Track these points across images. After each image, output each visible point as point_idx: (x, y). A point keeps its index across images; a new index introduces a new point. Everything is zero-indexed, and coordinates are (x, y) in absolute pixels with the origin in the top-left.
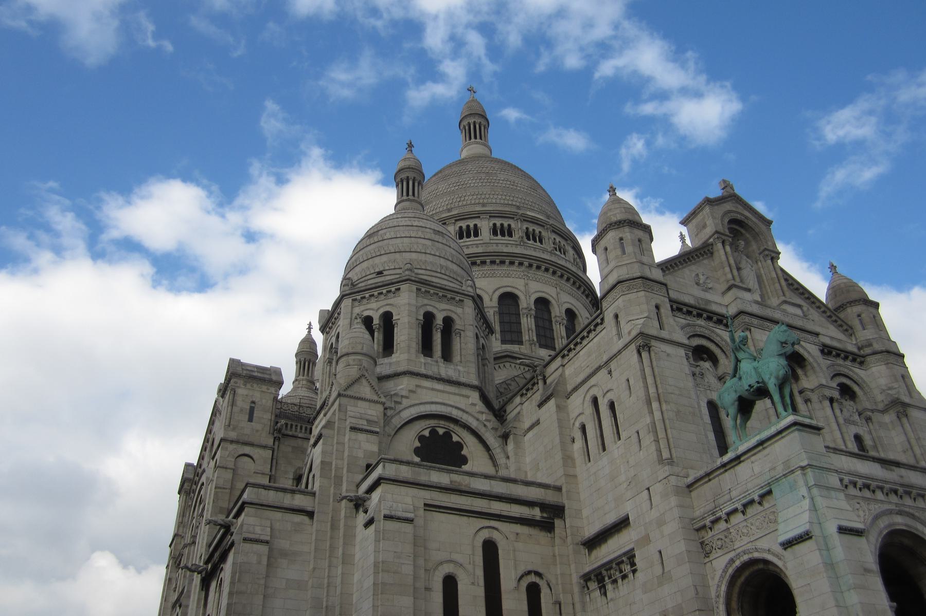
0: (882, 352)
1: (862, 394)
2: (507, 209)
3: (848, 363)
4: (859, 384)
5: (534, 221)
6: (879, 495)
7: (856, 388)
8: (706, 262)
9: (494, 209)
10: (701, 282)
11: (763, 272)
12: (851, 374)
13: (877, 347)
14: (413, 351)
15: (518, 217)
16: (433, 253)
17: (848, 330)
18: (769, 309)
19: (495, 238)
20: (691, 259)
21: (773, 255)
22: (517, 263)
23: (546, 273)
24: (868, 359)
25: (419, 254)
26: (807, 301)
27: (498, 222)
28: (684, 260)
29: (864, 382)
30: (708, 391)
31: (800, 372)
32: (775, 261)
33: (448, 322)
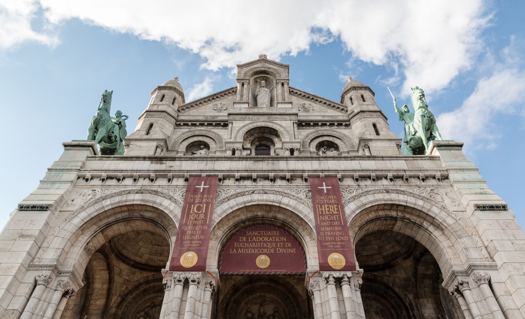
0: (358, 113)
1: (342, 143)
4: (340, 138)
7: (337, 141)
8: (229, 98)
10: (219, 108)
11: (275, 92)
12: (334, 134)
13: (356, 111)
21: (282, 81)
24: (351, 121)
26: (312, 100)
31: (276, 140)
32: (284, 84)
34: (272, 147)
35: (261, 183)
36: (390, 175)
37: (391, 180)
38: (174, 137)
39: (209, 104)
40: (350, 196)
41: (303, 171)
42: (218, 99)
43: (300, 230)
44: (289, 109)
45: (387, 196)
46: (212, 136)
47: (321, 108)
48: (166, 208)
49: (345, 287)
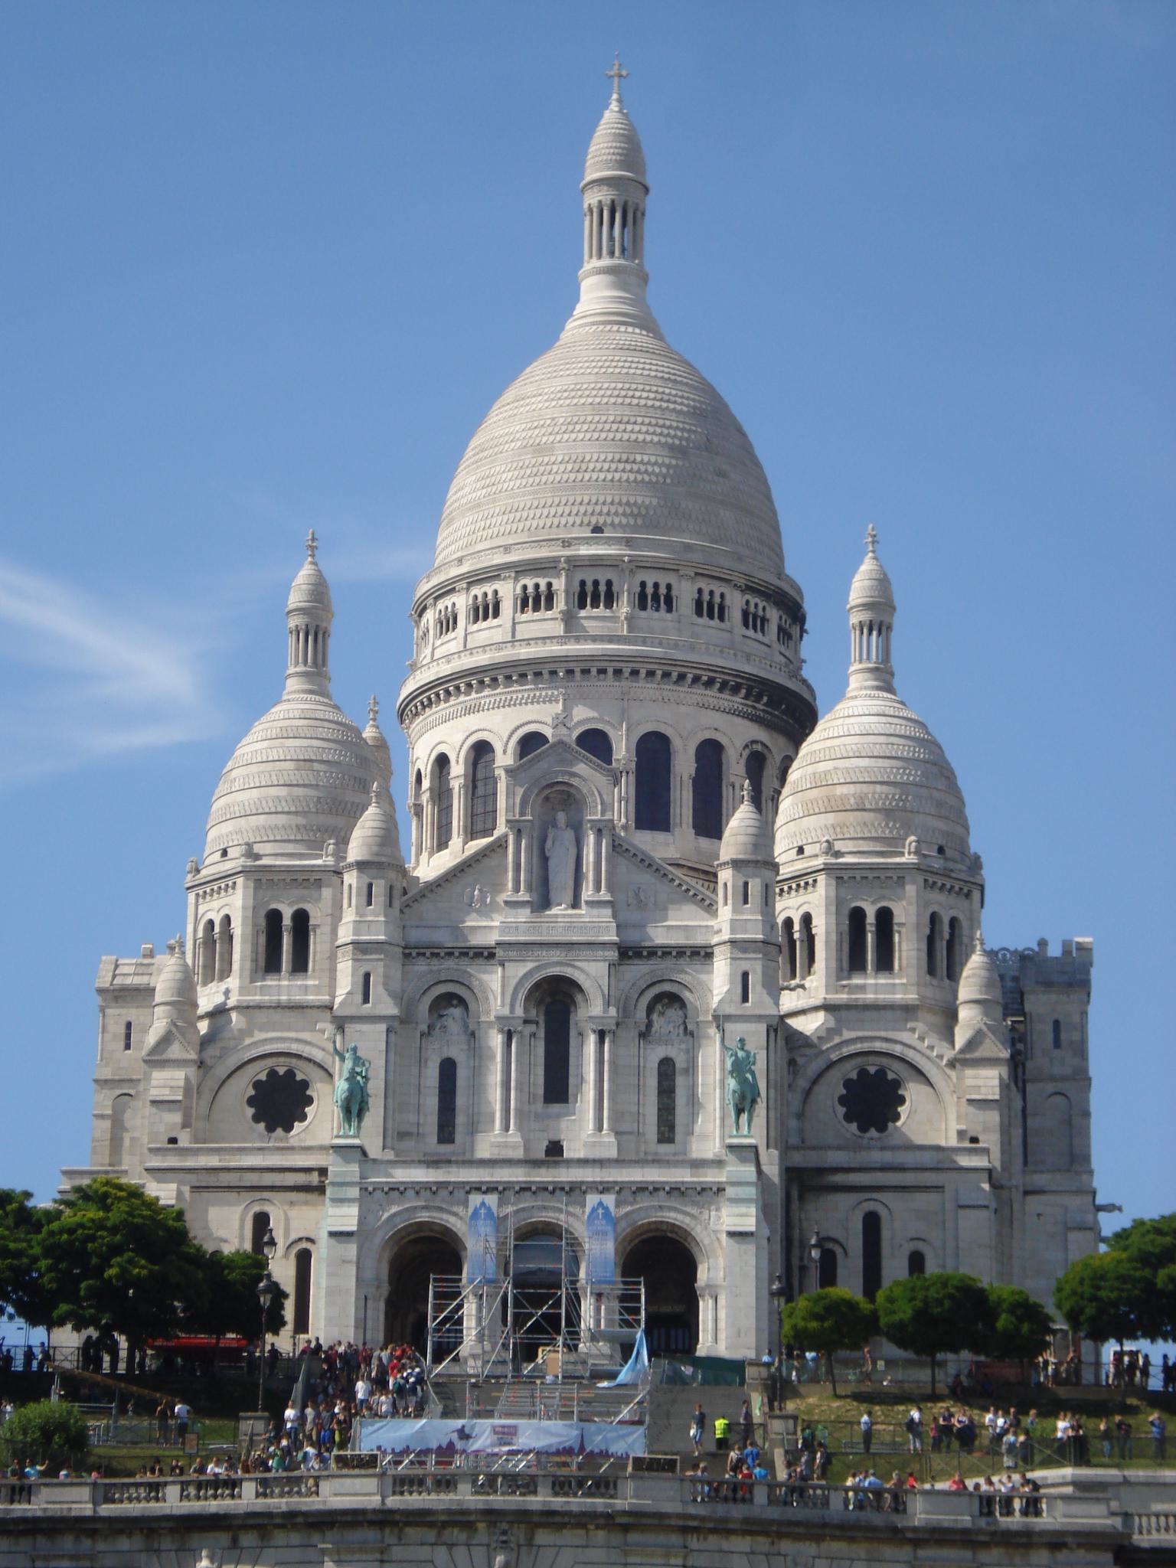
0: (725, 943)
3: (681, 961)
5: (595, 562)
7: (686, 995)
12: (680, 977)
14: (247, 973)
16: (286, 809)
19: (524, 617)
21: (599, 825)
22: (545, 672)
23: (602, 676)
24: (717, 951)
27: (530, 582)
30: (445, 1048)
31: (579, 998)
33: (301, 919)
34: (572, 1009)
36: (667, 1188)
41: (582, 1183)
49: (604, 1299)
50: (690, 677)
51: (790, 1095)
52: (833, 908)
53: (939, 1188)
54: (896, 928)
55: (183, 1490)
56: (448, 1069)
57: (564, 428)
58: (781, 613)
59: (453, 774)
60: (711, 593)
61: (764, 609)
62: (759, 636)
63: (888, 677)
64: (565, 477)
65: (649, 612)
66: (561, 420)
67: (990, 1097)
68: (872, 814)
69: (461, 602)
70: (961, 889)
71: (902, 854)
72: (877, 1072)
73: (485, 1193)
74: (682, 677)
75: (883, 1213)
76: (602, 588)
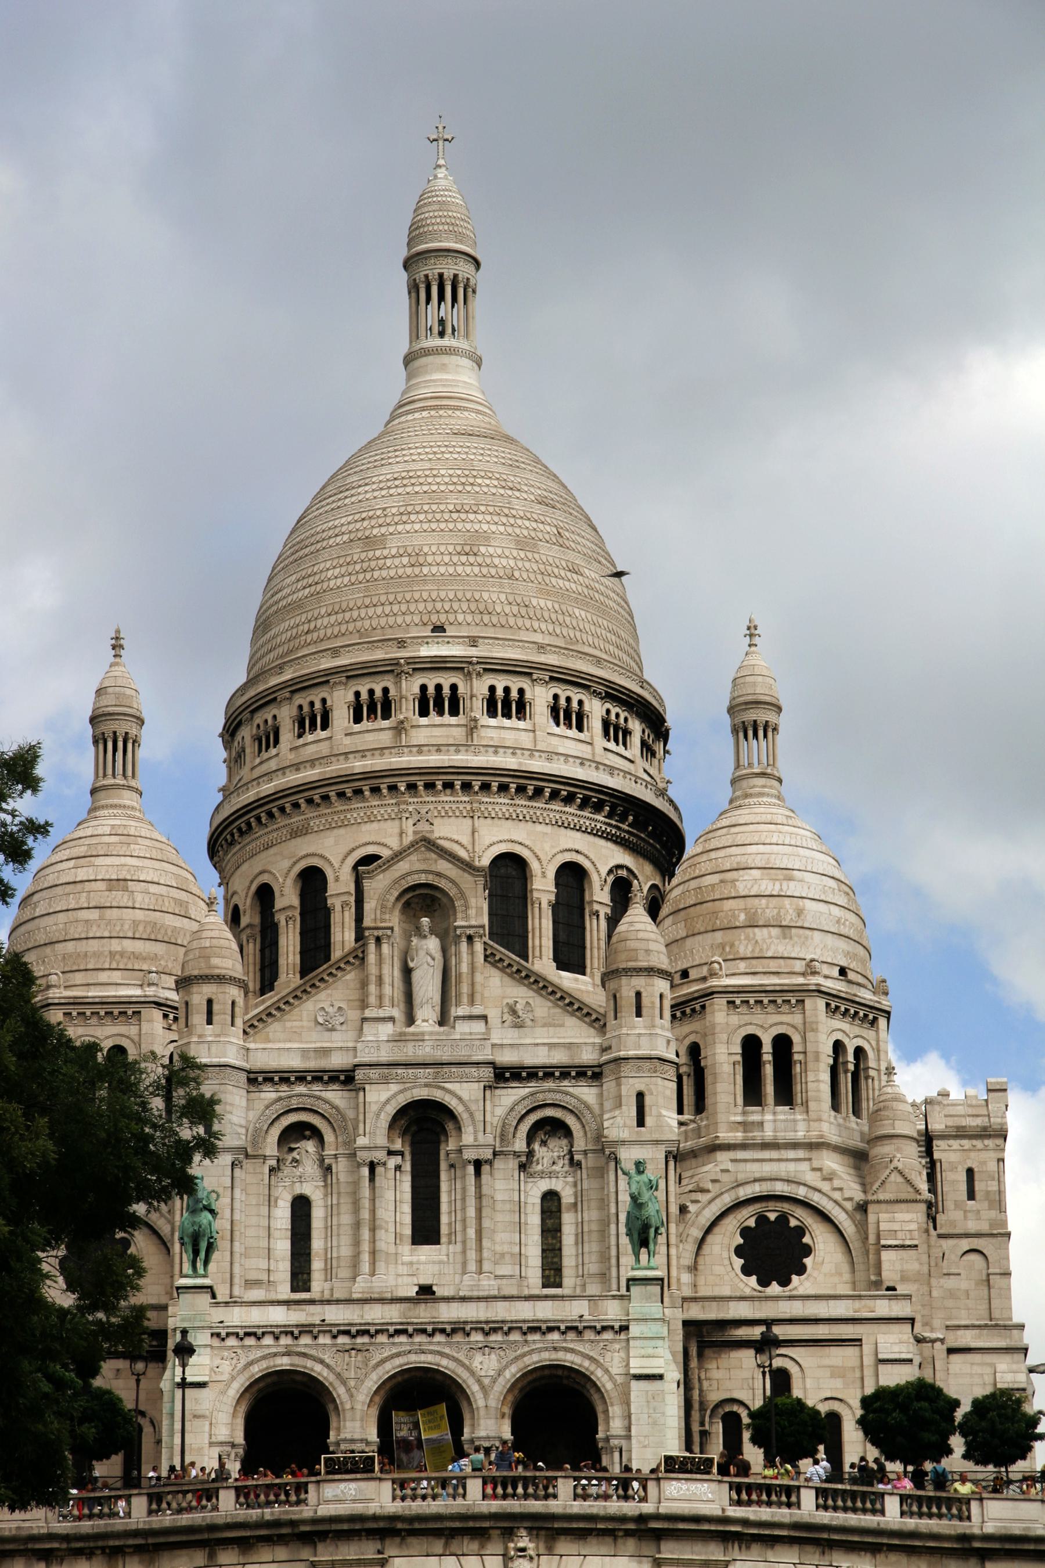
2: (379, 655)
5: (439, 665)
6: (268, 1340)
7: (571, 1121)
8: (348, 977)
9: (353, 661)
15: (398, 670)
16: (98, 935)
17: (597, 1021)
18: (410, 1045)
19: (357, 727)
20: (318, 984)
23: (448, 791)
24: (606, 1070)
25: (79, 943)
28: (305, 991)
29: (588, 1107)
30: (298, 1184)
31: (450, 1126)
34: (443, 1138)
35: (419, 1339)
36: (563, 1327)
37: (563, 1333)
38: (252, 1115)
39: (305, 1001)
40: (513, 1355)
41: (466, 1322)
42: (322, 985)
43: (459, 1394)
44: (478, 1043)
45: (554, 1355)
46: (325, 1111)
47: (553, 1011)
48: (319, 1374)
50: (547, 793)
51: (681, 1245)
52: (725, 1037)
53: (857, 1342)
54: (796, 1057)
55: (150, 1503)
56: (301, 1207)
57: (396, 519)
58: (643, 725)
59: (279, 903)
60: (568, 700)
61: (626, 720)
62: (620, 749)
63: (776, 783)
64: (400, 572)
65: (500, 721)
66: (394, 510)
67: (908, 1243)
68: (765, 930)
69: (285, 715)
70: (866, 1016)
71: (803, 974)
72: (777, 1218)
73: (354, 1337)
74: (538, 792)
75: (793, 1369)
76: (446, 691)
